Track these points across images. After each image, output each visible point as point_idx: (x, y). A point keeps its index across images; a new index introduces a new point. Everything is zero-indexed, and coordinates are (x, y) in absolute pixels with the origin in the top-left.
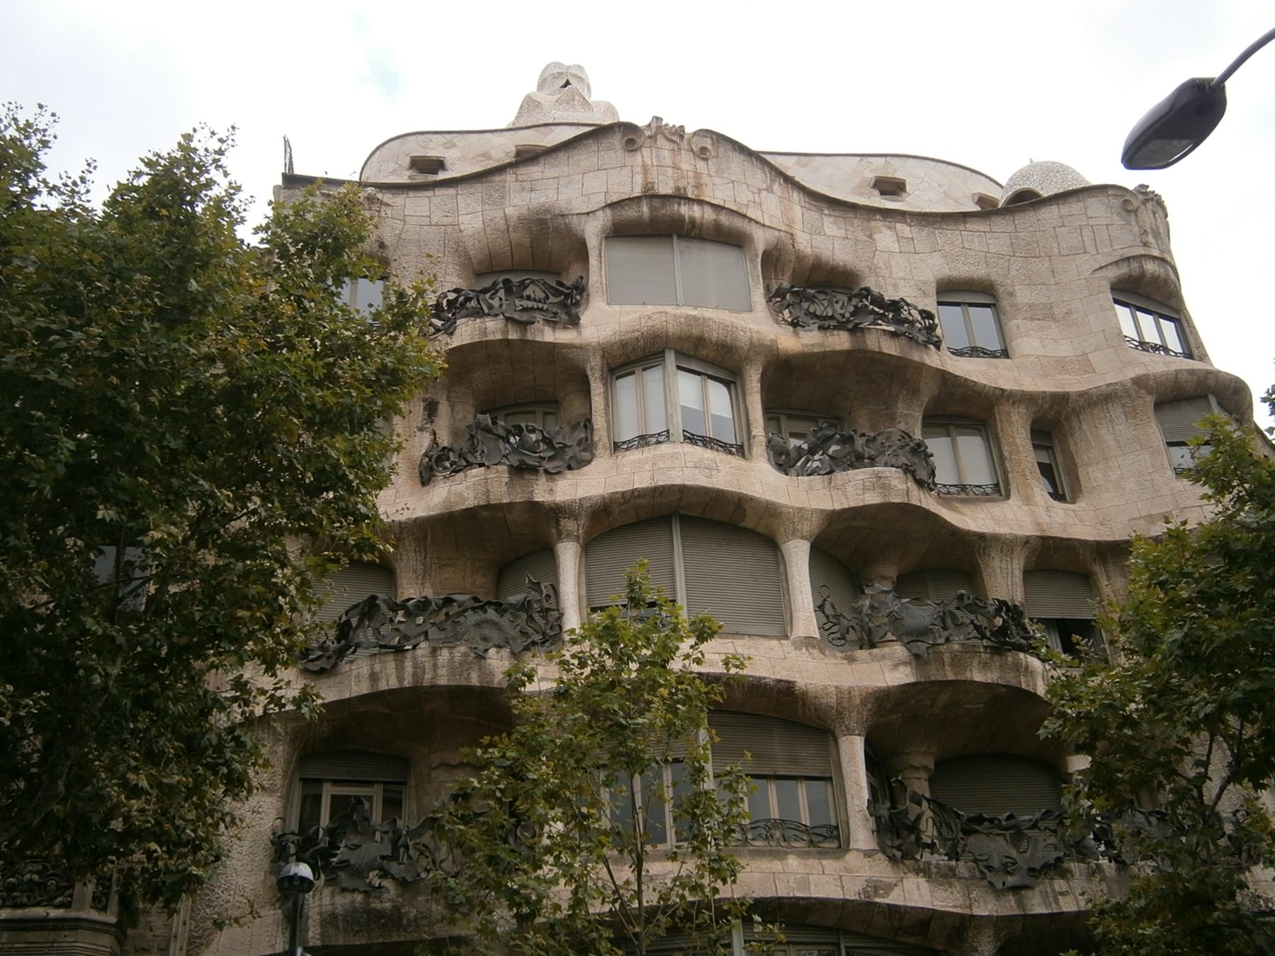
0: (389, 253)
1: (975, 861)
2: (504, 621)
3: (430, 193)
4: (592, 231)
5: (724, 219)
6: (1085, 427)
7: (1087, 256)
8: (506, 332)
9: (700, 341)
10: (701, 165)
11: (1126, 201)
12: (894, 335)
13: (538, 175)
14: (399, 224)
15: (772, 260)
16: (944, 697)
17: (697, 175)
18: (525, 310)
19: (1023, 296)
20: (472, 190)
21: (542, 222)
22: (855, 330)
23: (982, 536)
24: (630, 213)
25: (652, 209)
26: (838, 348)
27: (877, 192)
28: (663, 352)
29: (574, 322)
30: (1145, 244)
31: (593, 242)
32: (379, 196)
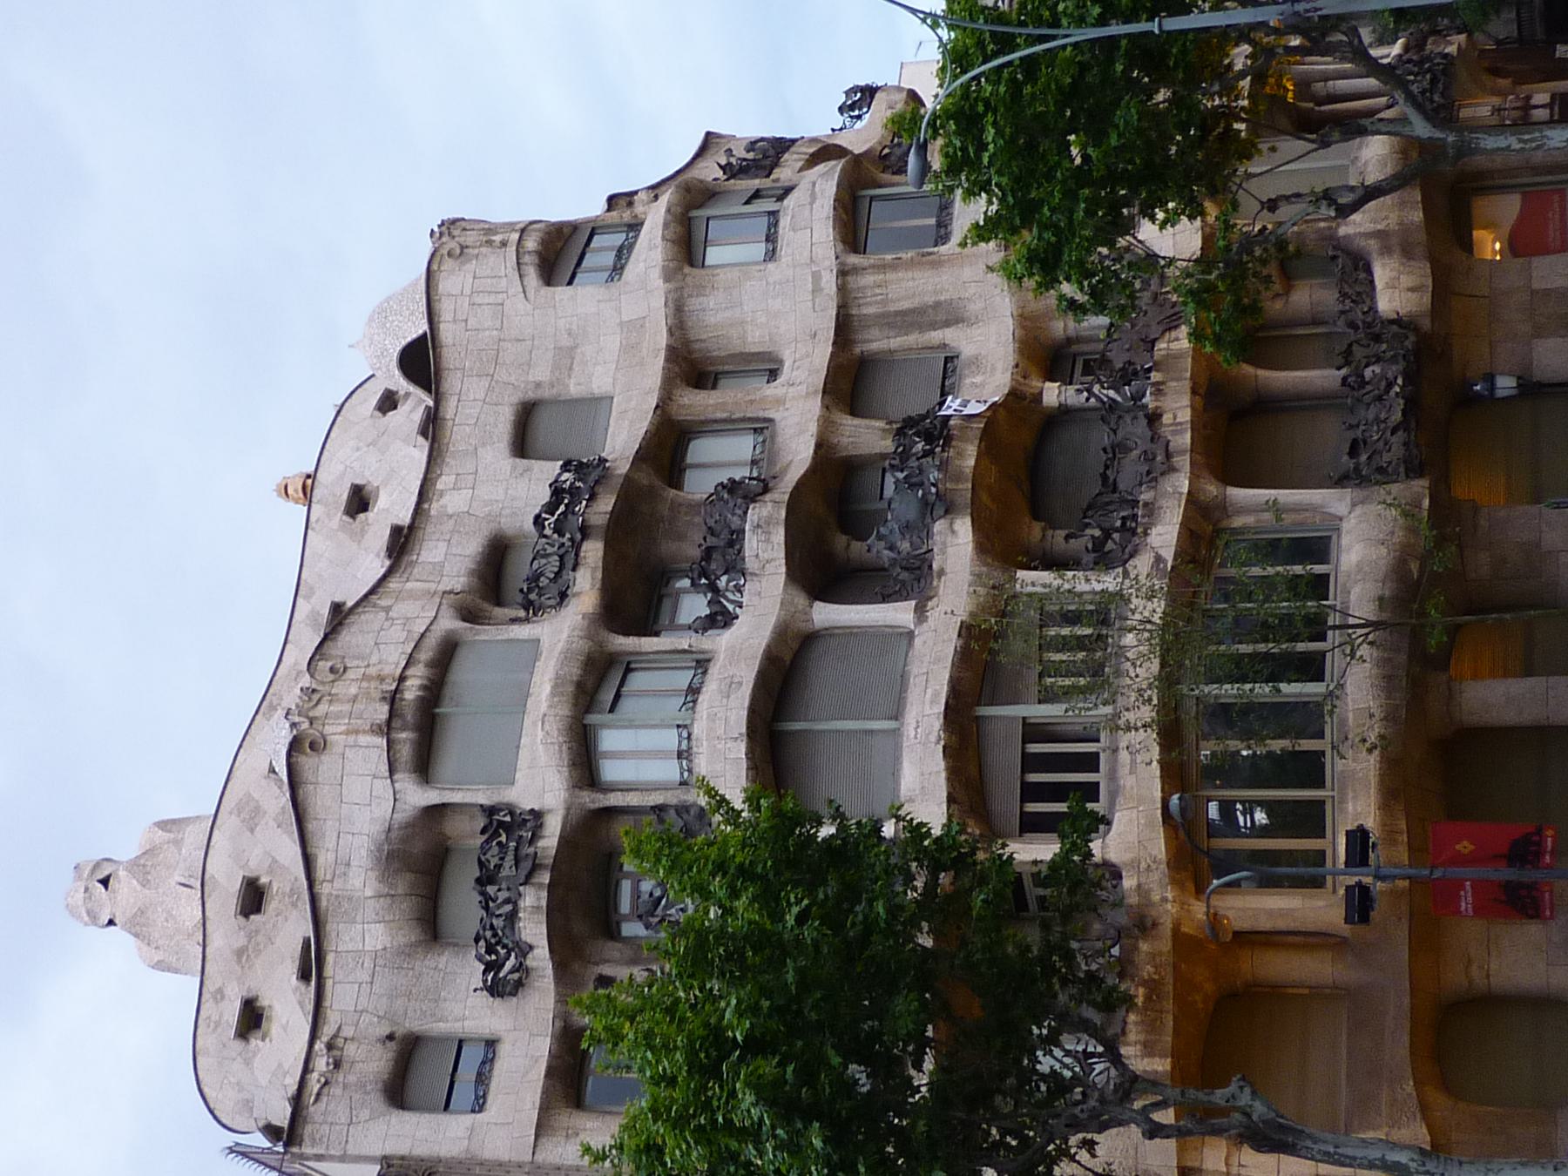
0: (400, 1032)
1: (1141, 484)
3: (329, 983)
4: (419, 797)
5: (425, 655)
6: (704, 337)
7: (507, 302)
8: (540, 885)
9: (580, 686)
10: (351, 675)
11: (449, 254)
13: (331, 857)
14: (365, 1018)
15: (470, 615)
16: (985, 497)
19: (541, 373)
20: (334, 935)
21: (391, 856)
22: (585, 531)
23: (818, 446)
24: (405, 753)
25: (403, 729)
26: (601, 554)
27: (362, 515)
28: (585, 726)
29: (537, 815)
30: (504, 244)
31: (432, 797)
32: (325, 1039)
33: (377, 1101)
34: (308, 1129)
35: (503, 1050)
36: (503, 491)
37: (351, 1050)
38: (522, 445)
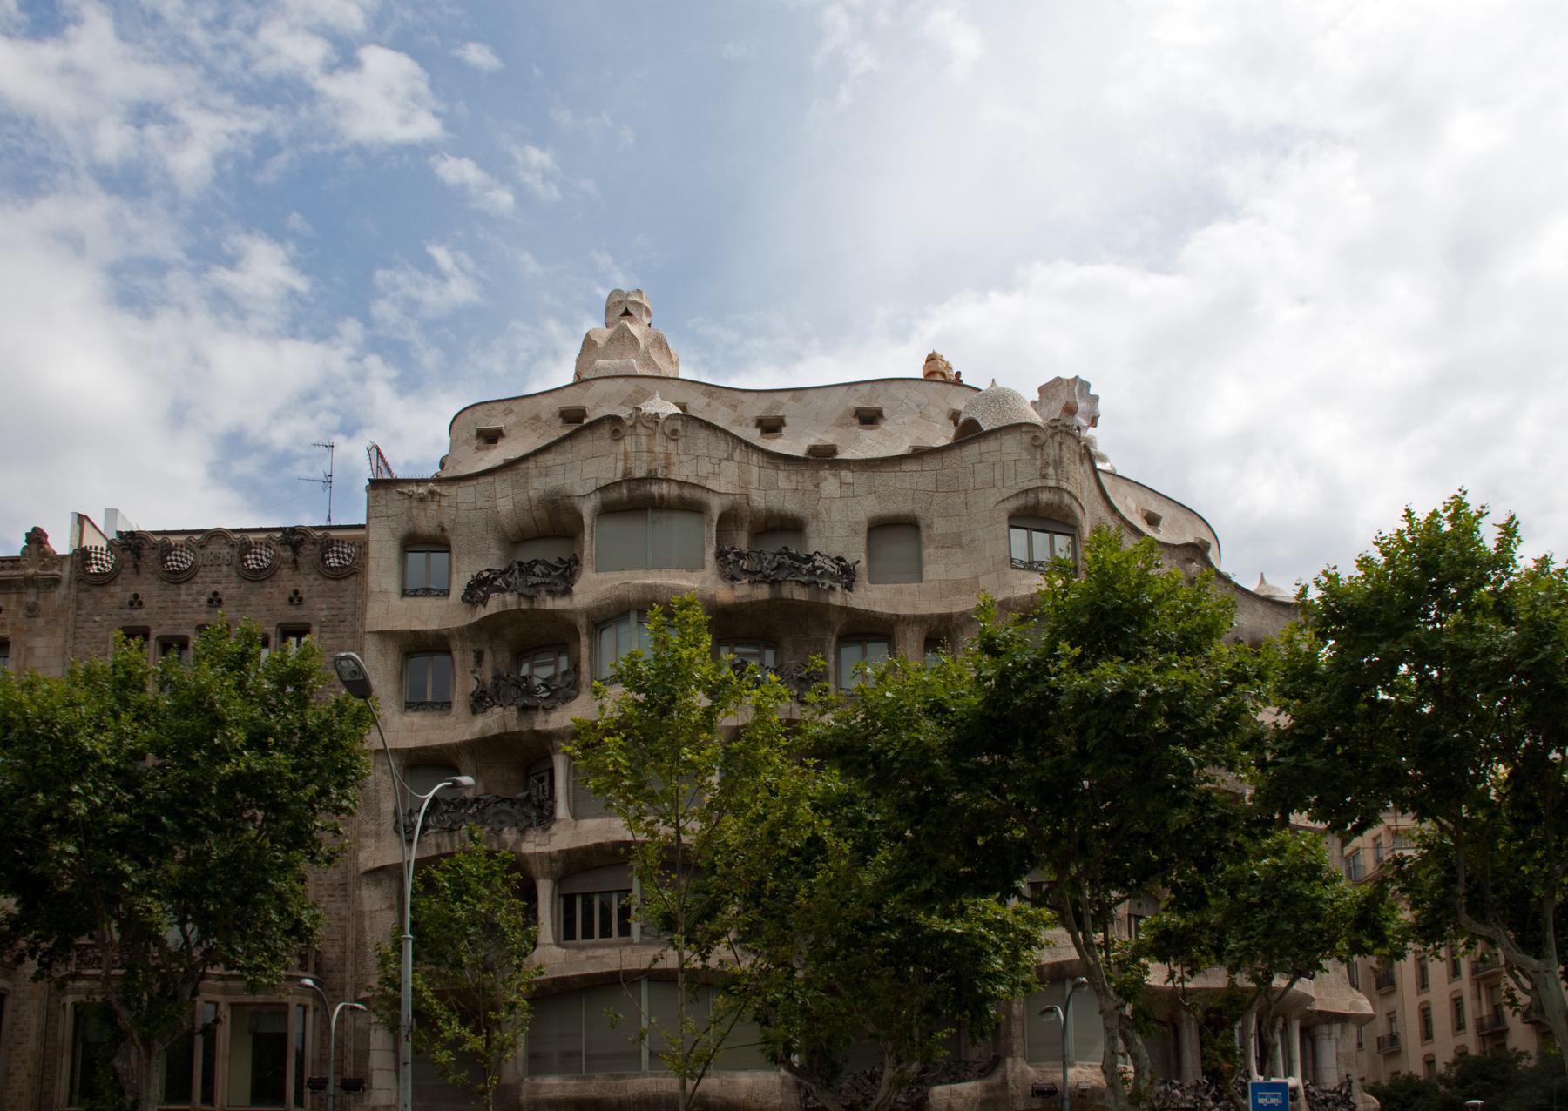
0: (448, 534)
2: (514, 811)
4: (587, 509)
5: (687, 493)
10: (672, 445)
12: (803, 584)
13: (550, 463)
15: (728, 520)
17: (668, 455)
18: (533, 585)
19: (940, 527)
21: (554, 502)
22: (774, 583)
24: (614, 495)
25: (629, 491)
29: (567, 592)
33: (402, 530)
34: (382, 492)
35: (442, 602)
36: (837, 523)
37: (433, 506)
38: (880, 527)
